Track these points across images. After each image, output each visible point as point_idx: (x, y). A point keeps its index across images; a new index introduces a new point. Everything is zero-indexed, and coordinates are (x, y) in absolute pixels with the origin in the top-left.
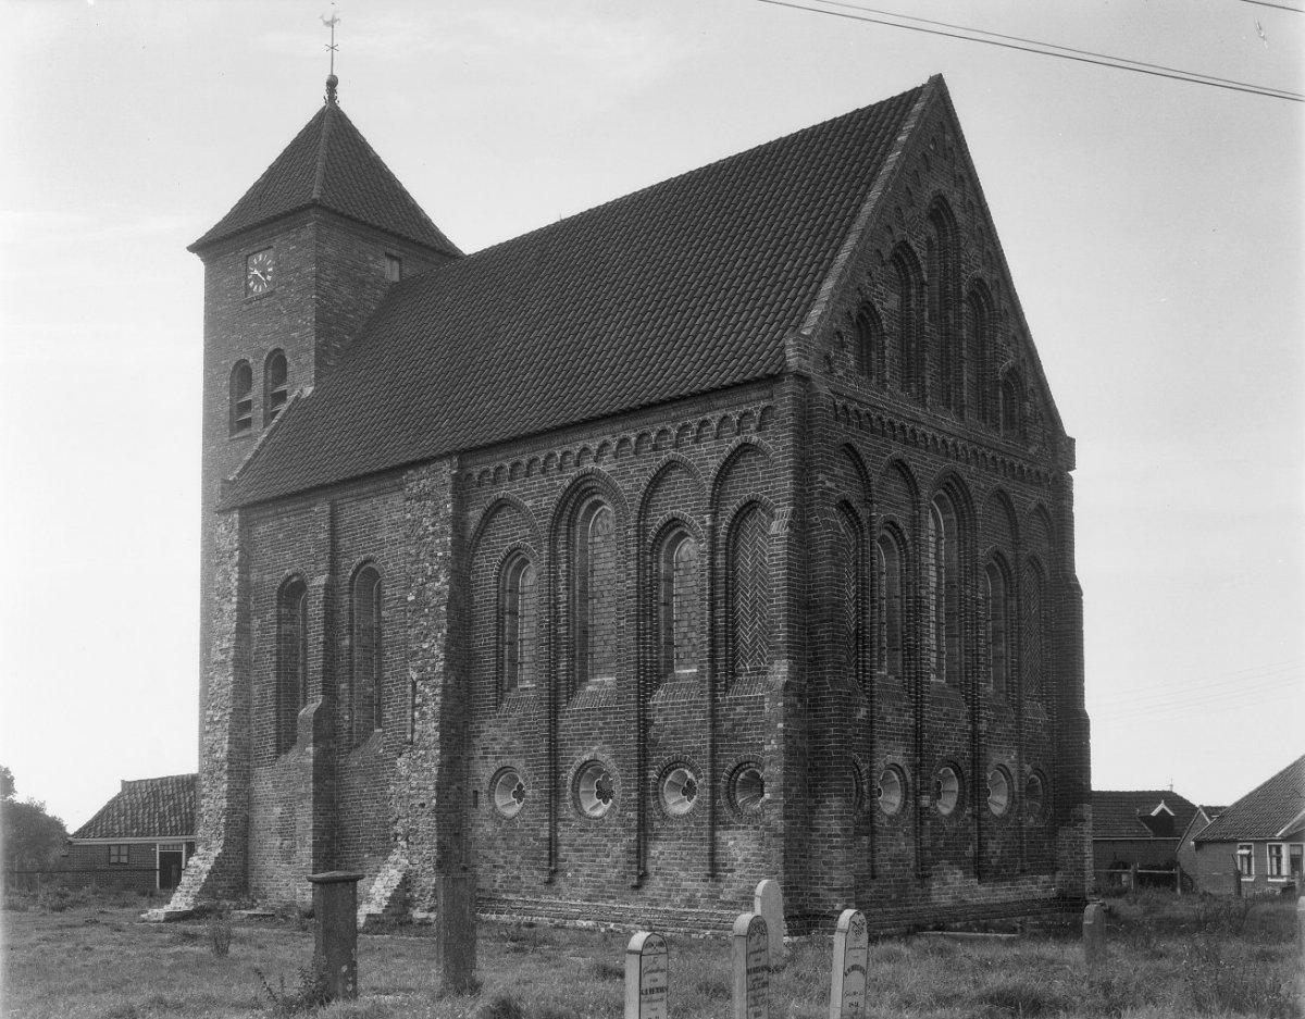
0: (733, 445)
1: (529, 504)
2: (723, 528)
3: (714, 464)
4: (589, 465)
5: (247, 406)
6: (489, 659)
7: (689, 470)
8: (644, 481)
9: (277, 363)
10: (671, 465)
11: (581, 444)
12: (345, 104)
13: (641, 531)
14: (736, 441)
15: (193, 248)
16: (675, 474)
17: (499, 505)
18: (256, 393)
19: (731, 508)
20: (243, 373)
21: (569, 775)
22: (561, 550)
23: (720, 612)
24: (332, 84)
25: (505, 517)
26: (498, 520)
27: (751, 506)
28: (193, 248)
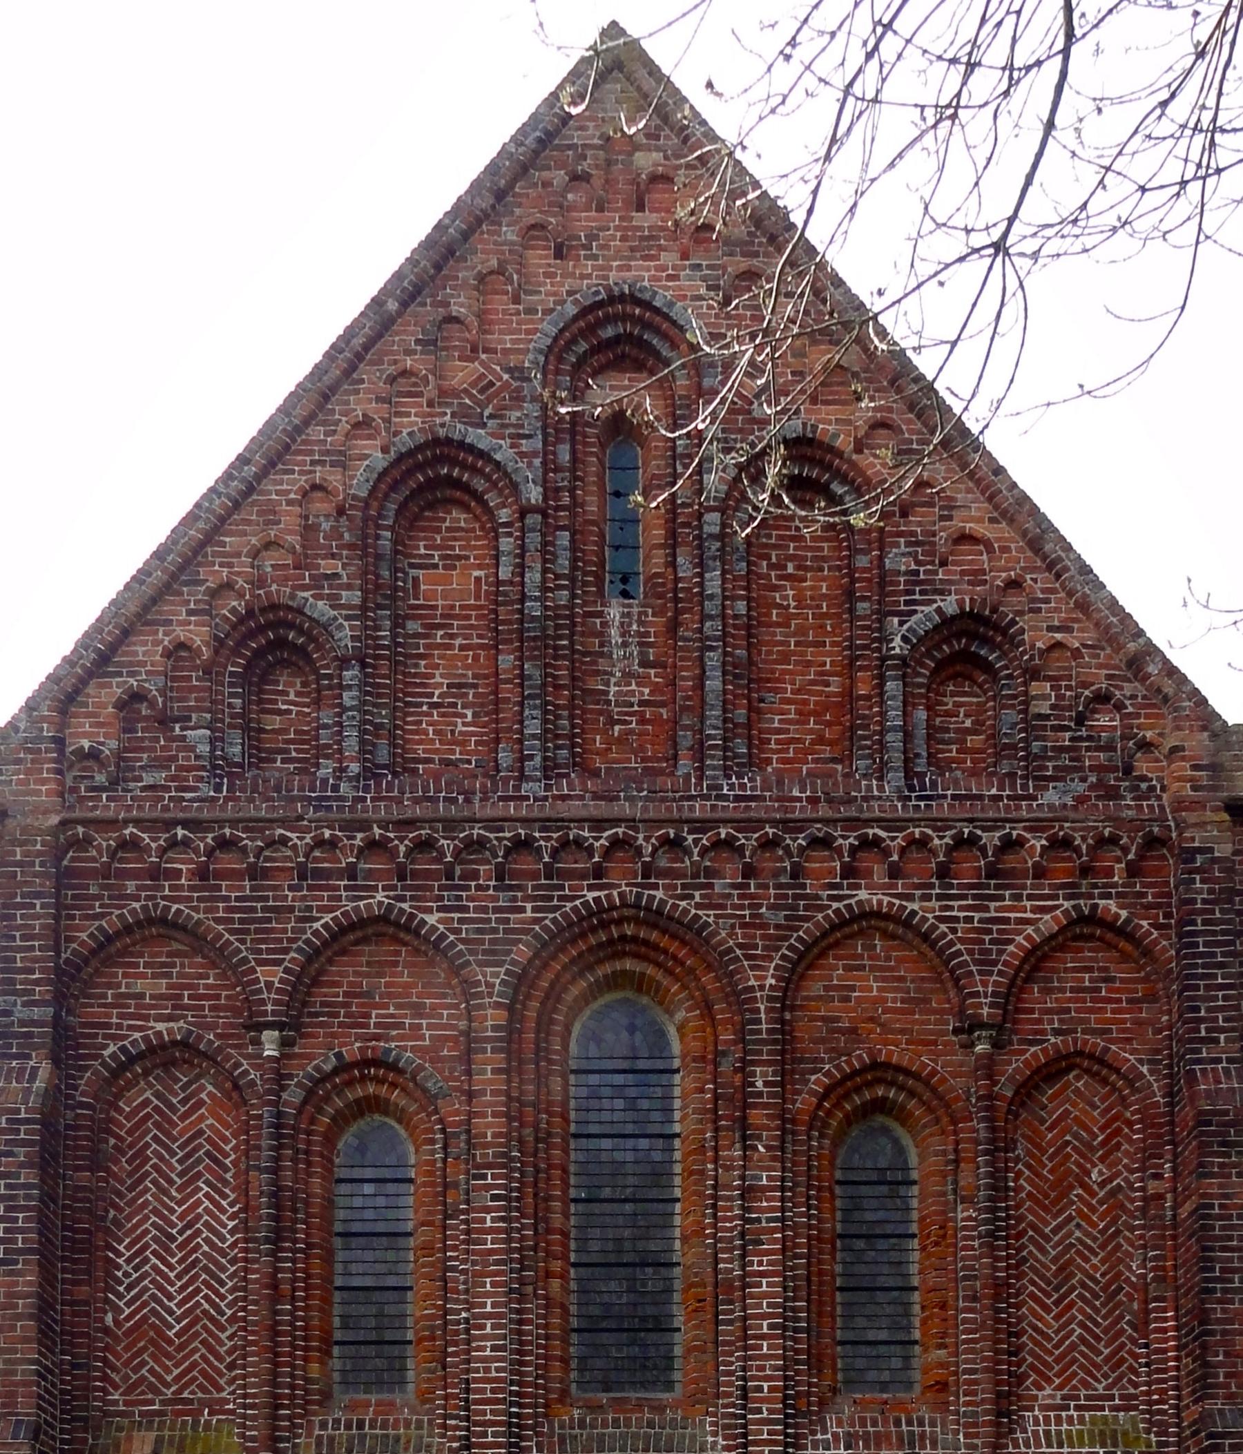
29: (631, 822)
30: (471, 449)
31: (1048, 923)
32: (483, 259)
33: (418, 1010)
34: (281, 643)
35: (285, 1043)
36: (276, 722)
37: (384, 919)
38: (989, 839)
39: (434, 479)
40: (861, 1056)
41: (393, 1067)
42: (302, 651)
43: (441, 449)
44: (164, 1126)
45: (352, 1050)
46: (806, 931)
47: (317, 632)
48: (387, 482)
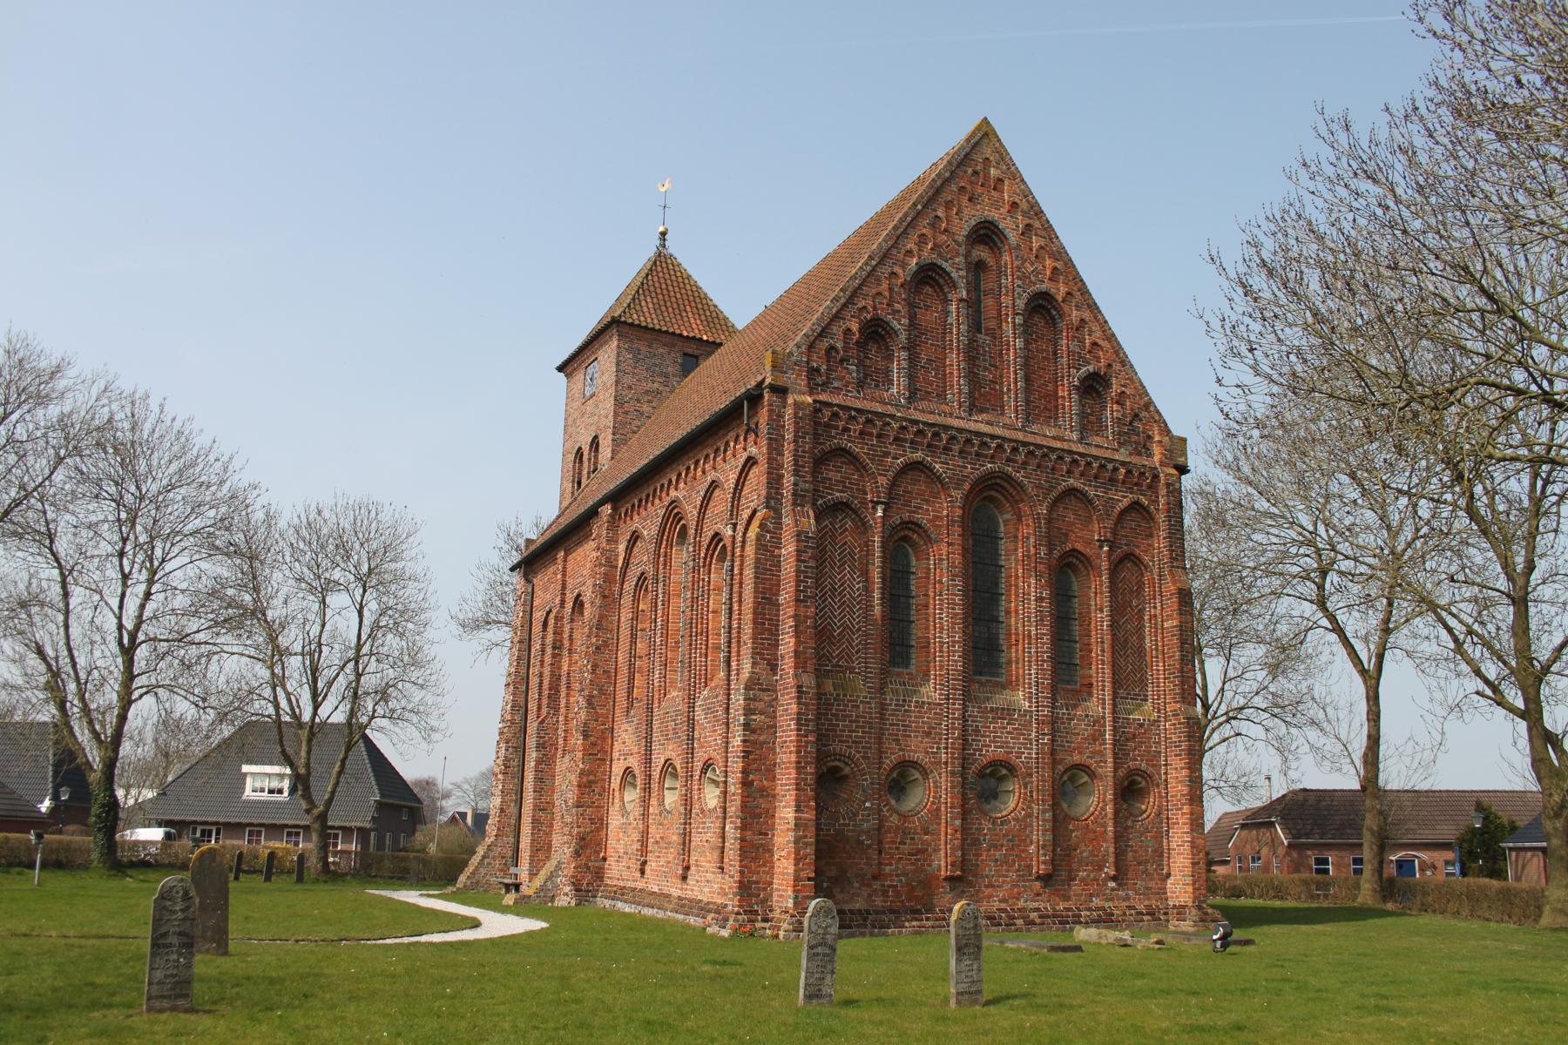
0: (742, 461)
3: (733, 477)
6: (624, 671)
12: (673, 247)
15: (560, 369)
19: (745, 515)
21: (656, 775)
23: (735, 616)
24: (663, 234)
26: (636, 550)
28: (560, 369)
29: (1004, 439)
30: (944, 270)
31: (1126, 502)
32: (945, 197)
33: (927, 501)
34: (876, 332)
35: (885, 511)
36: (868, 362)
37: (920, 463)
38: (1110, 466)
39: (929, 277)
40: (1069, 546)
41: (919, 526)
42: (883, 337)
43: (933, 267)
44: (833, 537)
45: (906, 516)
46: (1054, 494)
47: (892, 333)
48: (916, 274)
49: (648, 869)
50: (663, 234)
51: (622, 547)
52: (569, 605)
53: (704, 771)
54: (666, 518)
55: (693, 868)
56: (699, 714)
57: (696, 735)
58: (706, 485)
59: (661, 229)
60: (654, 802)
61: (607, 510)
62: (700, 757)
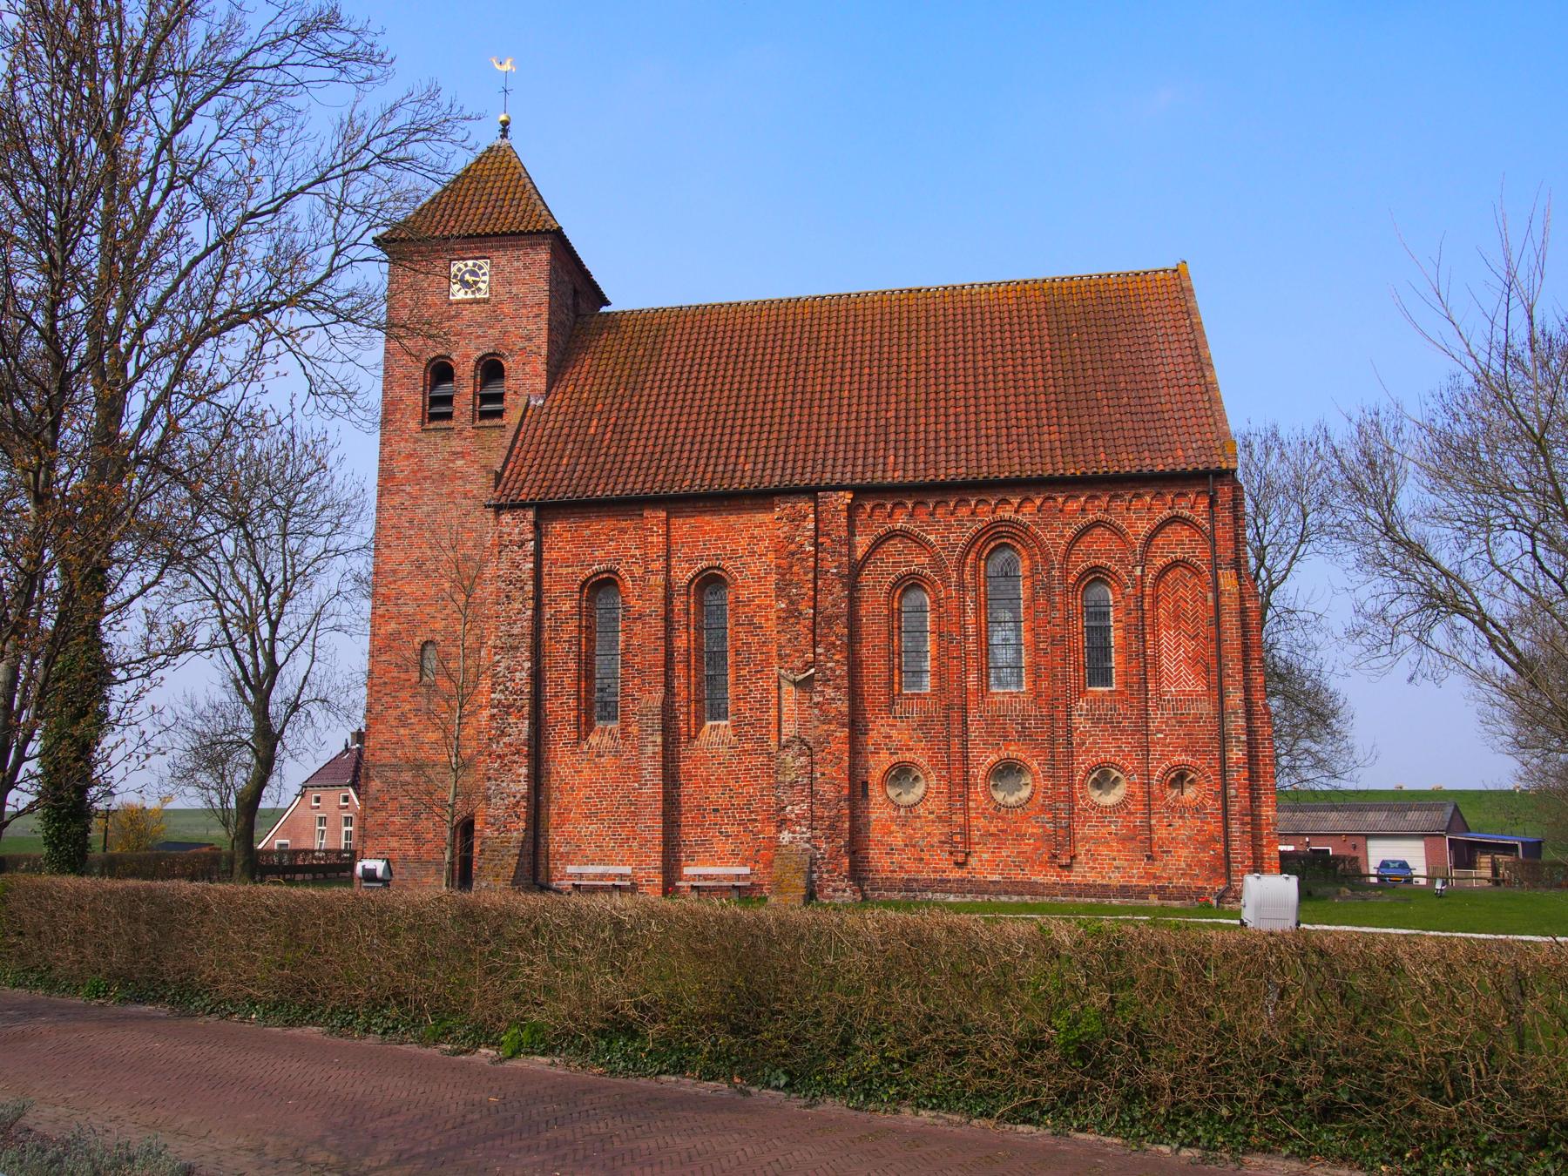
1: (932, 538)
2: (1149, 580)
3: (1143, 528)
4: (1007, 513)
5: (448, 400)
7: (1117, 531)
8: (1069, 533)
9: (491, 369)
10: (1097, 523)
11: (1000, 496)
13: (1066, 573)
14: (1167, 513)
16: (1098, 531)
17: (891, 535)
18: (464, 389)
19: (1159, 562)
20: (442, 371)
22: (967, 577)
24: (505, 124)
25: (894, 546)
27: (1175, 564)
49: (973, 861)
50: (505, 124)
51: (862, 542)
52: (683, 574)
53: (1089, 772)
54: (979, 534)
55: (1082, 858)
56: (1080, 723)
57: (1076, 740)
58: (1082, 522)
59: (503, 117)
60: (978, 797)
61: (848, 497)
62: (1083, 762)
